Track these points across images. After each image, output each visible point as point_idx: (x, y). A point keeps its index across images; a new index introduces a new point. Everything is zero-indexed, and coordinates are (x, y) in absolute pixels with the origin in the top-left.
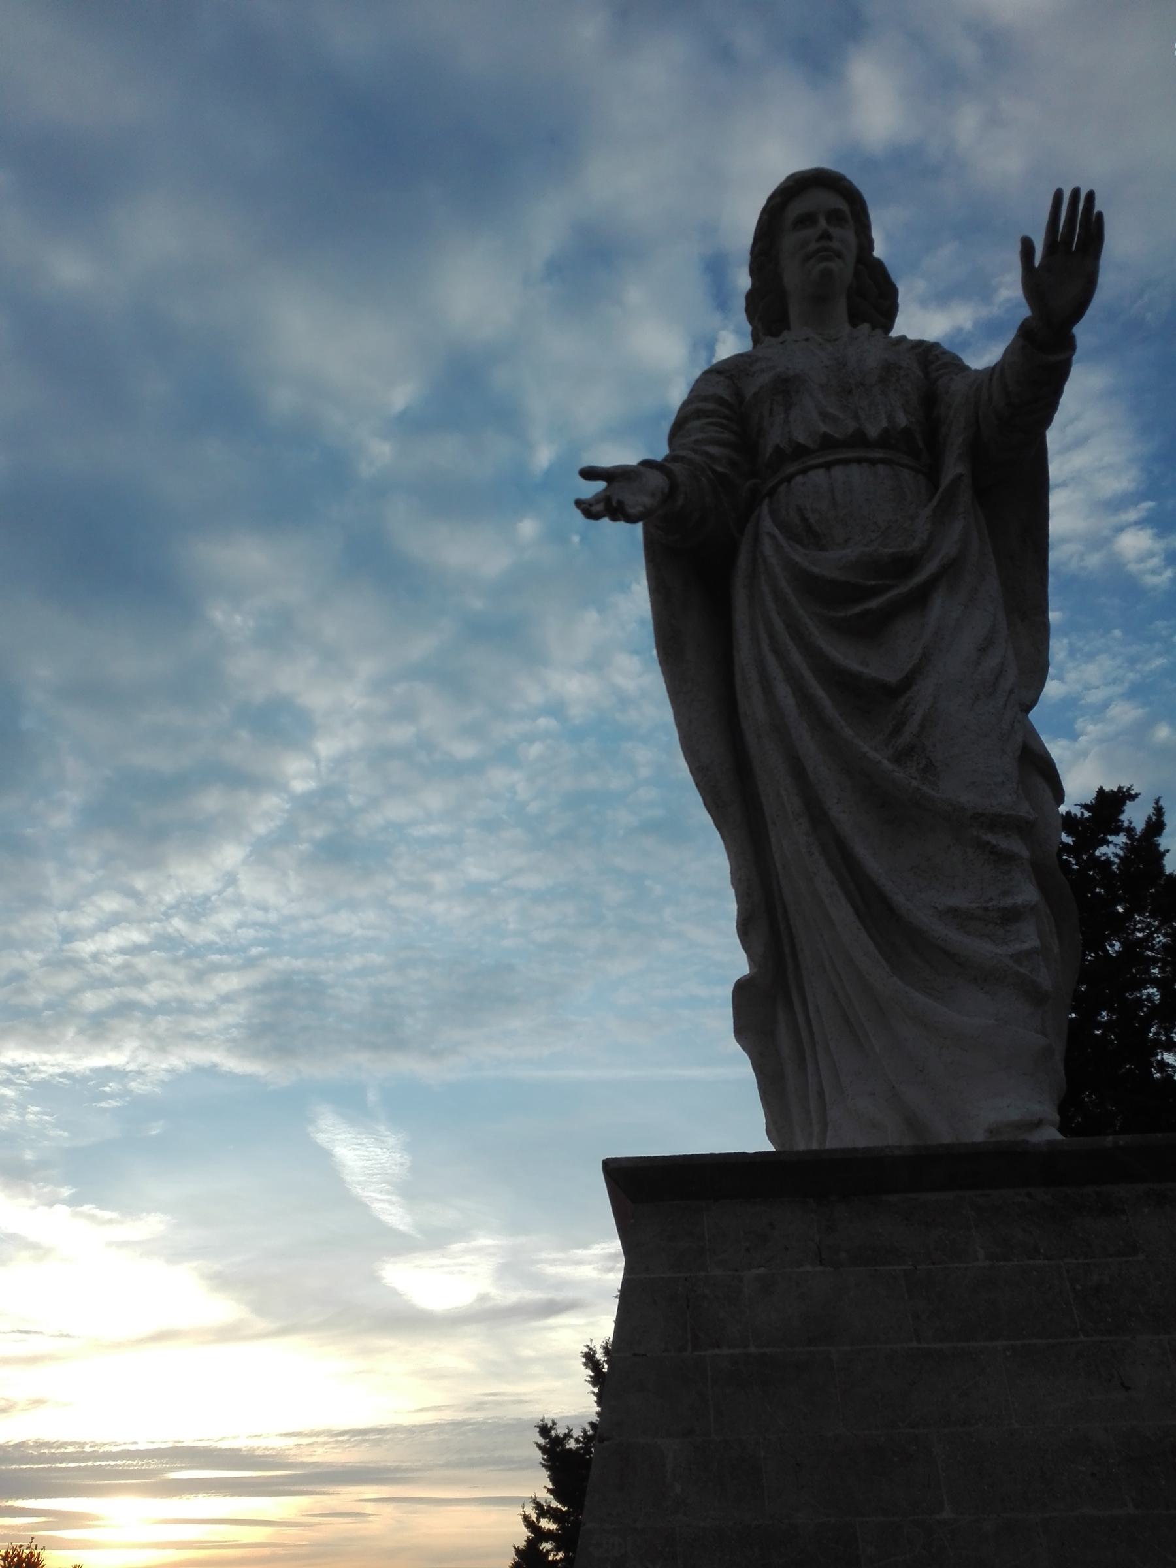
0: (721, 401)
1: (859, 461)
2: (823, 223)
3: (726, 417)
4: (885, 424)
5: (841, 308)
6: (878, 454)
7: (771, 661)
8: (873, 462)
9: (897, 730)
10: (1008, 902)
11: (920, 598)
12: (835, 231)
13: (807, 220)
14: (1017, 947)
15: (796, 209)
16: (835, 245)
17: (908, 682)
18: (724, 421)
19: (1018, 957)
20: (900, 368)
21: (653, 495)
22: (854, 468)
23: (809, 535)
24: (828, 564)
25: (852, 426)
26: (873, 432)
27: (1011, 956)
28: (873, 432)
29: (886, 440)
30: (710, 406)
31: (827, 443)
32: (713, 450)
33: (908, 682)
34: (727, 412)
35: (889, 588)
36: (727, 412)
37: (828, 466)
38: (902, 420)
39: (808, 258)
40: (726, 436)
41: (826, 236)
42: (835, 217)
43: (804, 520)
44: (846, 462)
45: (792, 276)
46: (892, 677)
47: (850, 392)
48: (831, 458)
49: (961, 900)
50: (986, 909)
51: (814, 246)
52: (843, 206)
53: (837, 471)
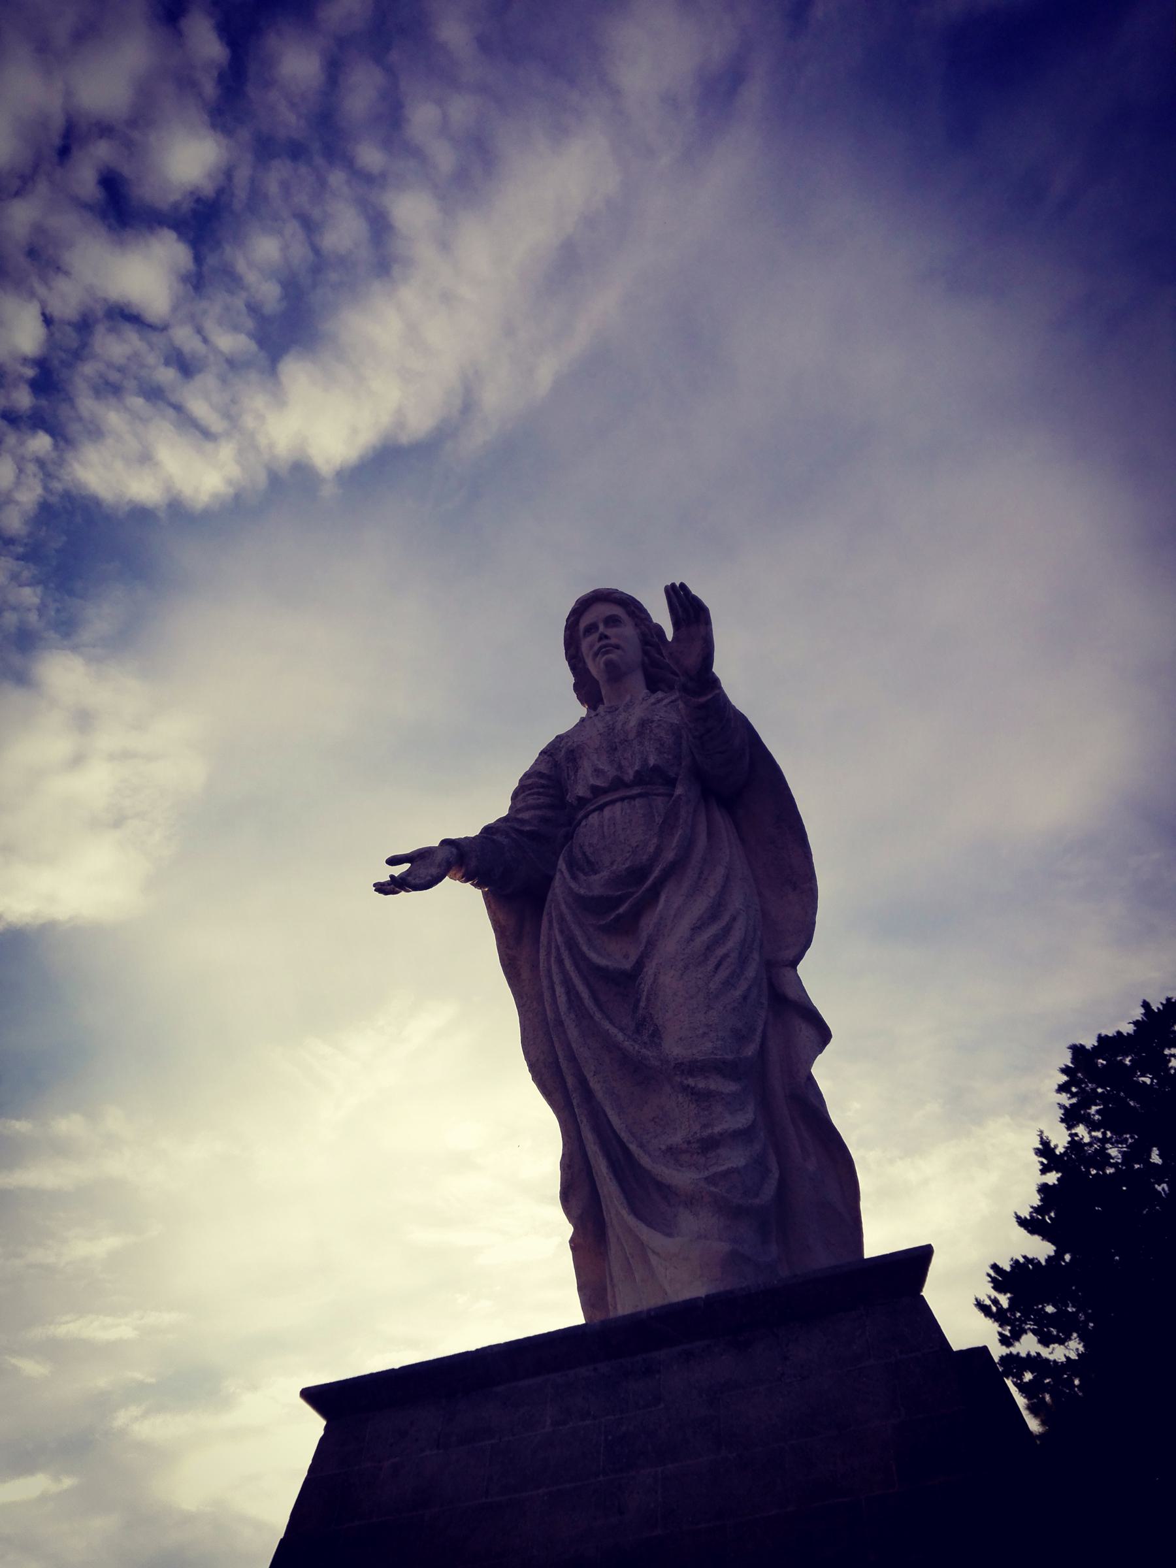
1: (622, 799)
2: (601, 628)
3: (543, 786)
4: (636, 768)
5: (637, 683)
6: (636, 791)
7: (555, 969)
8: (633, 798)
9: (636, 1007)
10: (706, 1133)
11: (654, 894)
12: (610, 632)
15: (584, 623)
16: (613, 641)
20: (652, 722)
22: (618, 804)
23: (583, 866)
24: (595, 885)
25: (612, 772)
27: (706, 1179)
28: (630, 775)
29: (639, 779)
30: (530, 781)
31: (596, 791)
32: (526, 815)
33: (640, 965)
34: (543, 781)
35: (633, 893)
36: (543, 781)
37: (601, 808)
38: (652, 762)
39: (596, 655)
40: (542, 800)
41: (603, 637)
42: (612, 621)
43: (584, 854)
44: (613, 802)
45: (595, 668)
46: (627, 965)
47: (616, 749)
48: (601, 802)
49: (677, 1139)
50: (689, 1143)
51: (598, 645)
52: (617, 611)
53: (607, 812)
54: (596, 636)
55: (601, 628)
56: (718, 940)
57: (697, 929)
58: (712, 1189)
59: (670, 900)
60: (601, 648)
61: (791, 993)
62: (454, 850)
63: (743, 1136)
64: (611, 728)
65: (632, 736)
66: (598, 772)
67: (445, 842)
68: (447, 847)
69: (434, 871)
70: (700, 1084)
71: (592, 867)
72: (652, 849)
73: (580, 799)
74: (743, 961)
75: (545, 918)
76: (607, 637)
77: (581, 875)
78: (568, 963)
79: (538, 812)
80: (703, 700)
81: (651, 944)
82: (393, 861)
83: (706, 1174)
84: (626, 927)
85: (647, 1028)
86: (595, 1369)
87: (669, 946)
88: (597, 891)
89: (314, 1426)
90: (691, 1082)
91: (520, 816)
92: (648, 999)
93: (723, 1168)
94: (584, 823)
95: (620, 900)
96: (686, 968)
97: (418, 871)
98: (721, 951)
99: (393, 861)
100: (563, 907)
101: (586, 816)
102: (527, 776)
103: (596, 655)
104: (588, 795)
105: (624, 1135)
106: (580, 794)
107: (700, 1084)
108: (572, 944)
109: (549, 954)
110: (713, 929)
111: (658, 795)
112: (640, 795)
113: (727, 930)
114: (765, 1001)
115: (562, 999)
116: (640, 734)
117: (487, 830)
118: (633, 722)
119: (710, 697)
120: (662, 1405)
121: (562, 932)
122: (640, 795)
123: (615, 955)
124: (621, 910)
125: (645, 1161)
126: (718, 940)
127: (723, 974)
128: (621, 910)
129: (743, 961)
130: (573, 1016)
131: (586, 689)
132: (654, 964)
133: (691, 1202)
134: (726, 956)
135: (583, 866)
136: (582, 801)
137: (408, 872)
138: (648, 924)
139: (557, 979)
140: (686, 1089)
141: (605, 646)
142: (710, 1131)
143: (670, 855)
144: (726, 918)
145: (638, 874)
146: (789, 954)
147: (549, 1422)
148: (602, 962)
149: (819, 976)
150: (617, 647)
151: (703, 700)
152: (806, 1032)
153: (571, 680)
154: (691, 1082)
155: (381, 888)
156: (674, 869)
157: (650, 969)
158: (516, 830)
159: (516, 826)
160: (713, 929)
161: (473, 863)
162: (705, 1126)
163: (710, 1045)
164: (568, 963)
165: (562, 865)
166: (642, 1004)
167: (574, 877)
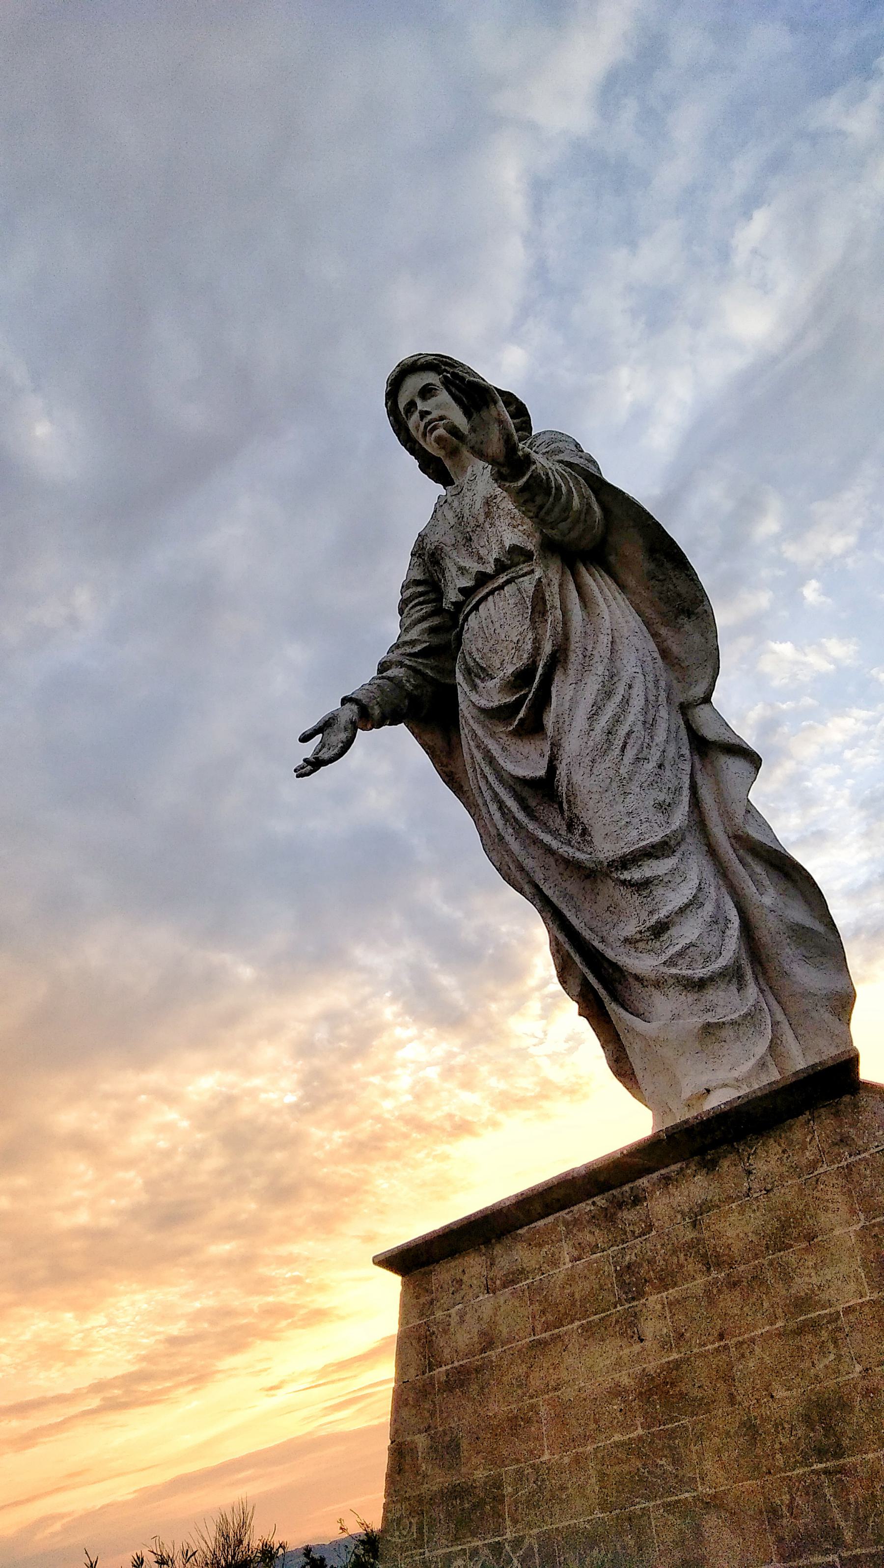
0: (417, 583)
1: (492, 593)
2: (419, 402)
3: (421, 594)
8: (501, 587)
9: (562, 811)
13: (412, 405)
14: (672, 951)
15: (402, 405)
17: (552, 769)
18: (421, 599)
19: (671, 962)
21: (346, 730)
22: (490, 598)
23: (478, 674)
24: (492, 694)
26: (490, 569)
28: (490, 569)
29: (501, 567)
31: (466, 592)
32: (414, 634)
33: (552, 769)
34: (420, 589)
35: (526, 695)
36: (420, 589)
37: (476, 608)
41: (424, 414)
42: (426, 392)
44: (484, 598)
45: (430, 446)
48: (474, 602)
50: (641, 932)
51: (422, 424)
54: (416, 416)
55: (419, 402)
56: (617, 720)
57: (593, 717)
58: (674, 971)
59: (562, 691)
60: (425, 427)
61: (710, 733)
62: (355, 708)
63: (694, 903)
64: (460, 517)
65: (481, 519)
66: (462, 570)
67: (345, 701)
68: (348, 705)
69: (343, 736)
70: (635, 874)
71: (485, 673)
72: (529, 646)
73: (452, 603)
74: (650, 725)
75: (463, 736)
76: (428, 413)
77: (478, 681)
78: (491, 779)
79: (425, 625)
80: (521, 482)
81: (556, 745)
82: (305, 738)
83: (664, 957)
84: (533, 727)
85: (576, 828)
86: (594, 1203)
87: (572, 745)
88: (497, 699)
89: (393, 1282)
90: (626, 875)
91: (407, 638)
92: (569, 802)
93: (678, 948)
94: (466, 627)
95: (516, 706)
96: (593, 761)
97: (328, 743)
98: (623, 731)
99: (305, 738)
100: (471, 722)
101: (466, 619)
102: (405, 587)
103: (424, 435)
104: (461, 598)
105: (586, 934)
106: (454, 600)
107: (635, 874)
108: (491, 760)
109: (475, 770)
110: (611, 709)
111: (523, 575)
112: (508, 582)
113: (626, 701)
114: (686, 751)
115: (497, 816)
116: (488, 515)
117: (383, 667)
118: (478, 505)
119: (525, 479)
120: (654, 1233)
121: (478, 747)
122: (508, 582)
123: (527, 762)
124: (521, 715)
125: (610, 954)
126: (617, 720)
127: (630, 753)
128: (521, 715)
129: (650, 725)
130: (510, 831)
131: (434, 469)
132: (564, 762)
133: (658, 984)
134: (629, 734)
135: (478, 674)
136: (459, 606)
137: (323, 745)
138: (549, 720)
139: (488, 795)
140: (624, 883)
141: (430, 423)
142: (656, 917)
143: (547, 648)
144: (621, 689)
145: (523, 677)
146: (698, 691)
147: (567, 1260)
148: (520, 772)
149: (736, 705)
150: (442, 418)
151: (521, 482)
152: (734, 766)
153: (413, 462)
154: (626, 875)
155: (301, 773)
156: (558, 658)
157: (562, 770)
158: (410, 655)
159: (409, 650)
160: (611, 709)
161: (376, 711)
162: (651, 913)
163: (635, 833)
164: (491, 779)
165: (459, 678)
166: (565, 806)
167: (474, 687)
